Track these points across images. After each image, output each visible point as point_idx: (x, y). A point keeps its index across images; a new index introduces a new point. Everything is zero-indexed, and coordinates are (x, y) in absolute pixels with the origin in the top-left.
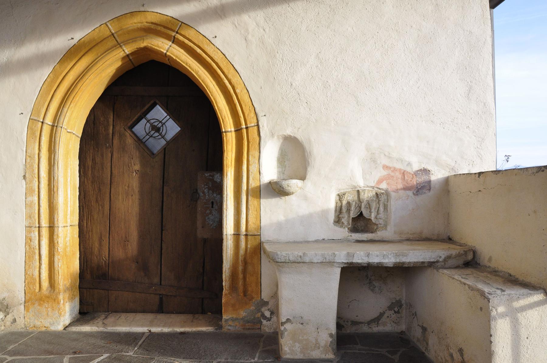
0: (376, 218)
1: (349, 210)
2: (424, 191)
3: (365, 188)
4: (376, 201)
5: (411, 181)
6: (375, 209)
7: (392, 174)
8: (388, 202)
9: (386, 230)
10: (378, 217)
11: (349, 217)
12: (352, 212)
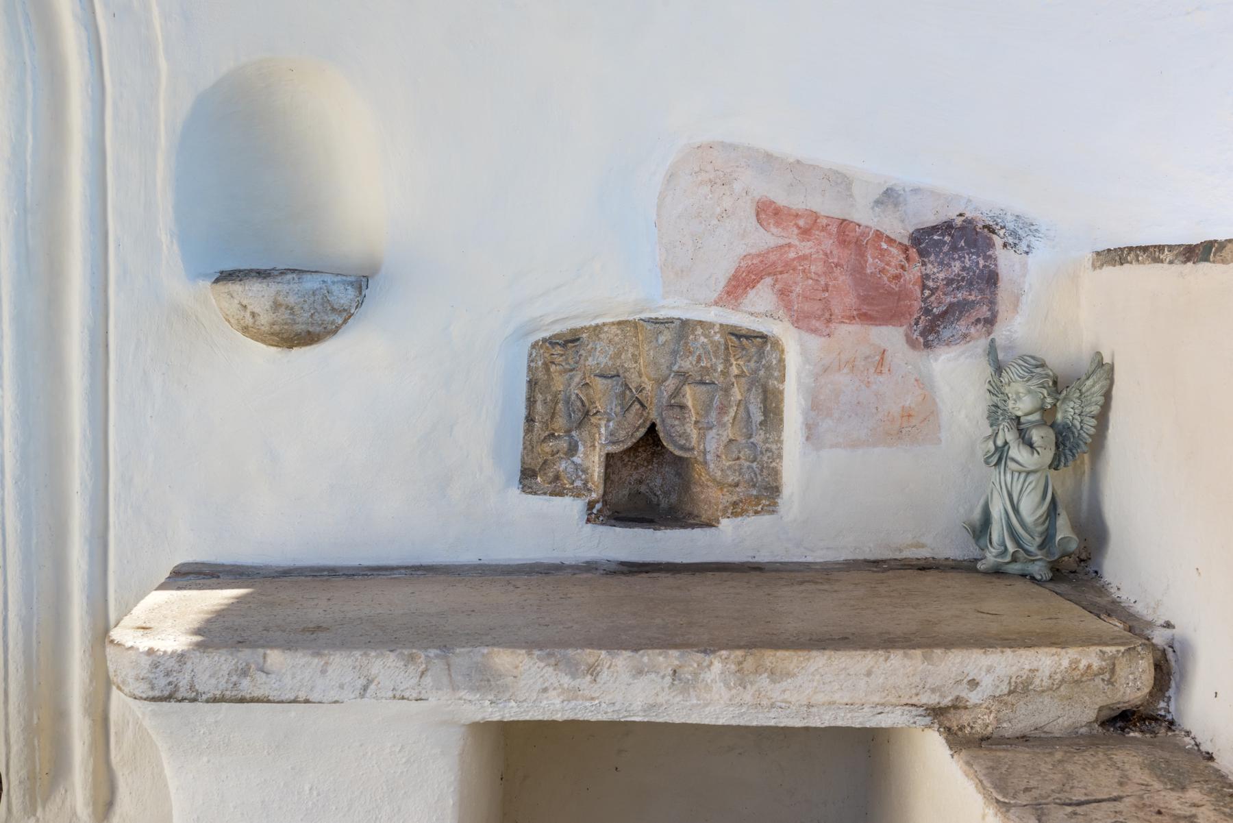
2: (961, 327)
5: (897, 277)
8: (782, 379)
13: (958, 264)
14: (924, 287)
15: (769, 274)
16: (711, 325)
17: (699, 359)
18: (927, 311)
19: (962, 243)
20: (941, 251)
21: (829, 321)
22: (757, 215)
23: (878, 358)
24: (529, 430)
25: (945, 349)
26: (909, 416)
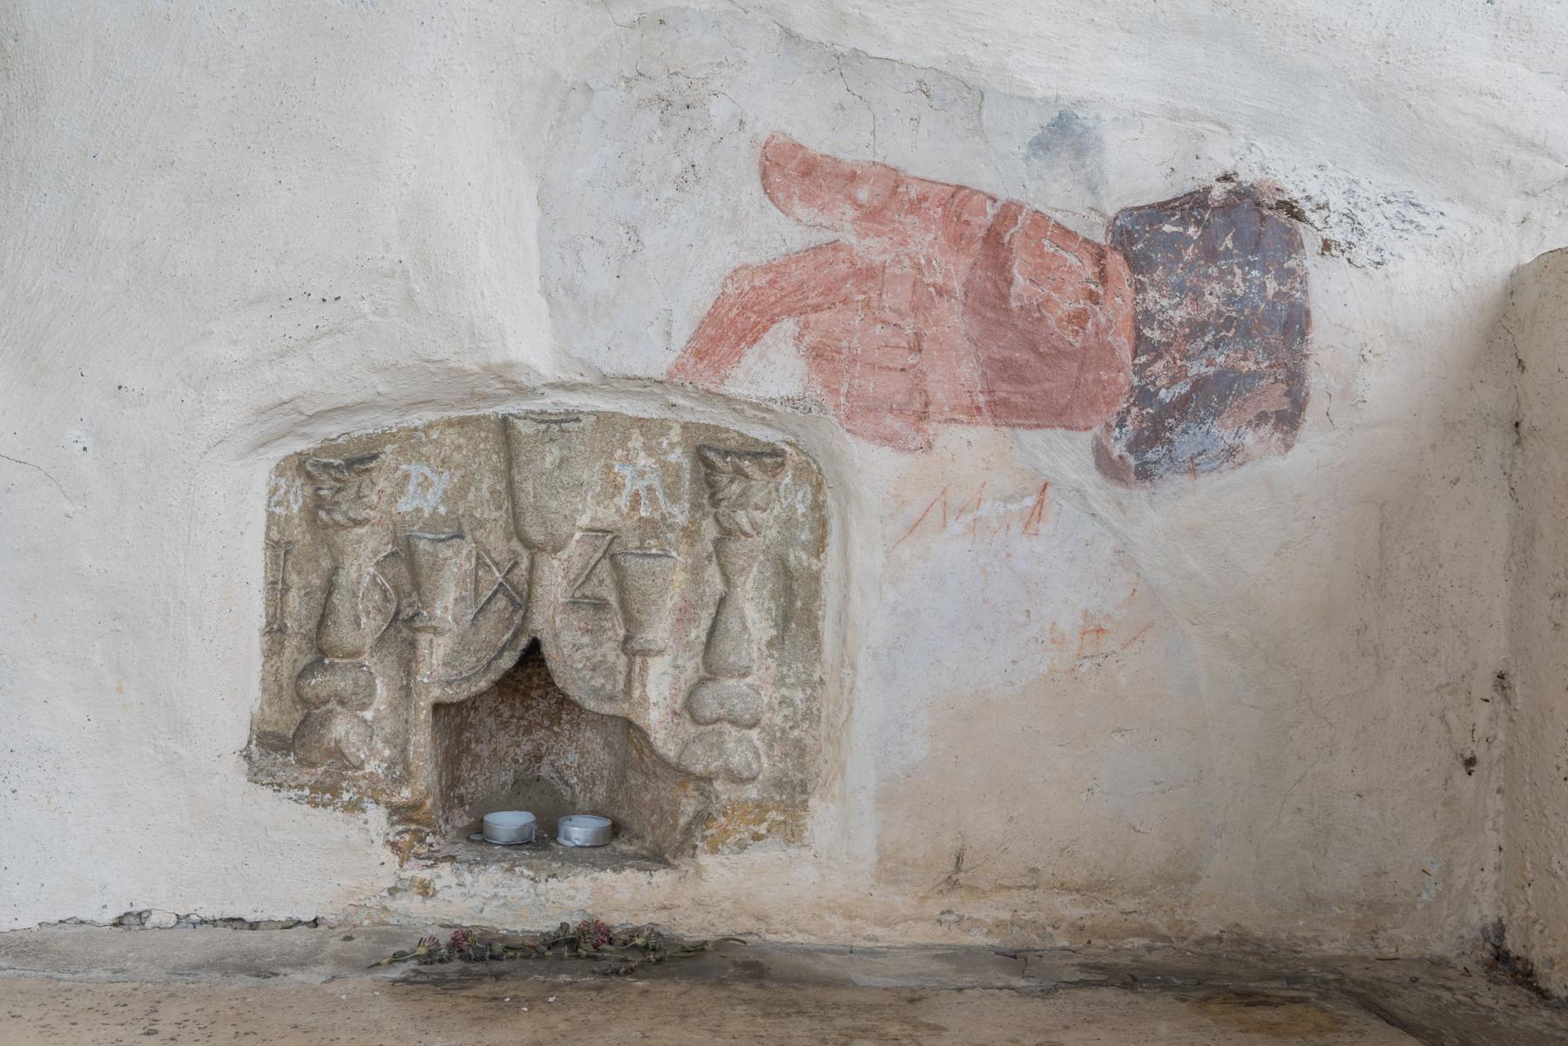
0: (689, 708)
1: (403, 629)
2: (1222, 432)
3: (573, 401)
4: (691, 534)
5: (1079, 318)
6: (685, 615)
7: (872, 248)
8: (819, 546)
9: (792, 833)
10: (709, 703)
11: (407, 691)
12: (435, 654)
13: (1218, 288)
14: (1141, 344)
15: (789, 312)
16: (663, 427)
17: (636, 500)
18: (1144, 396)
19: (1229, 243)
20: (1179, 256)
21: (923, 416)
22: (764, 176)
23: (1030, 502)
24: (273, 650)
25: (1184, 480)
26: (1100, 630)
